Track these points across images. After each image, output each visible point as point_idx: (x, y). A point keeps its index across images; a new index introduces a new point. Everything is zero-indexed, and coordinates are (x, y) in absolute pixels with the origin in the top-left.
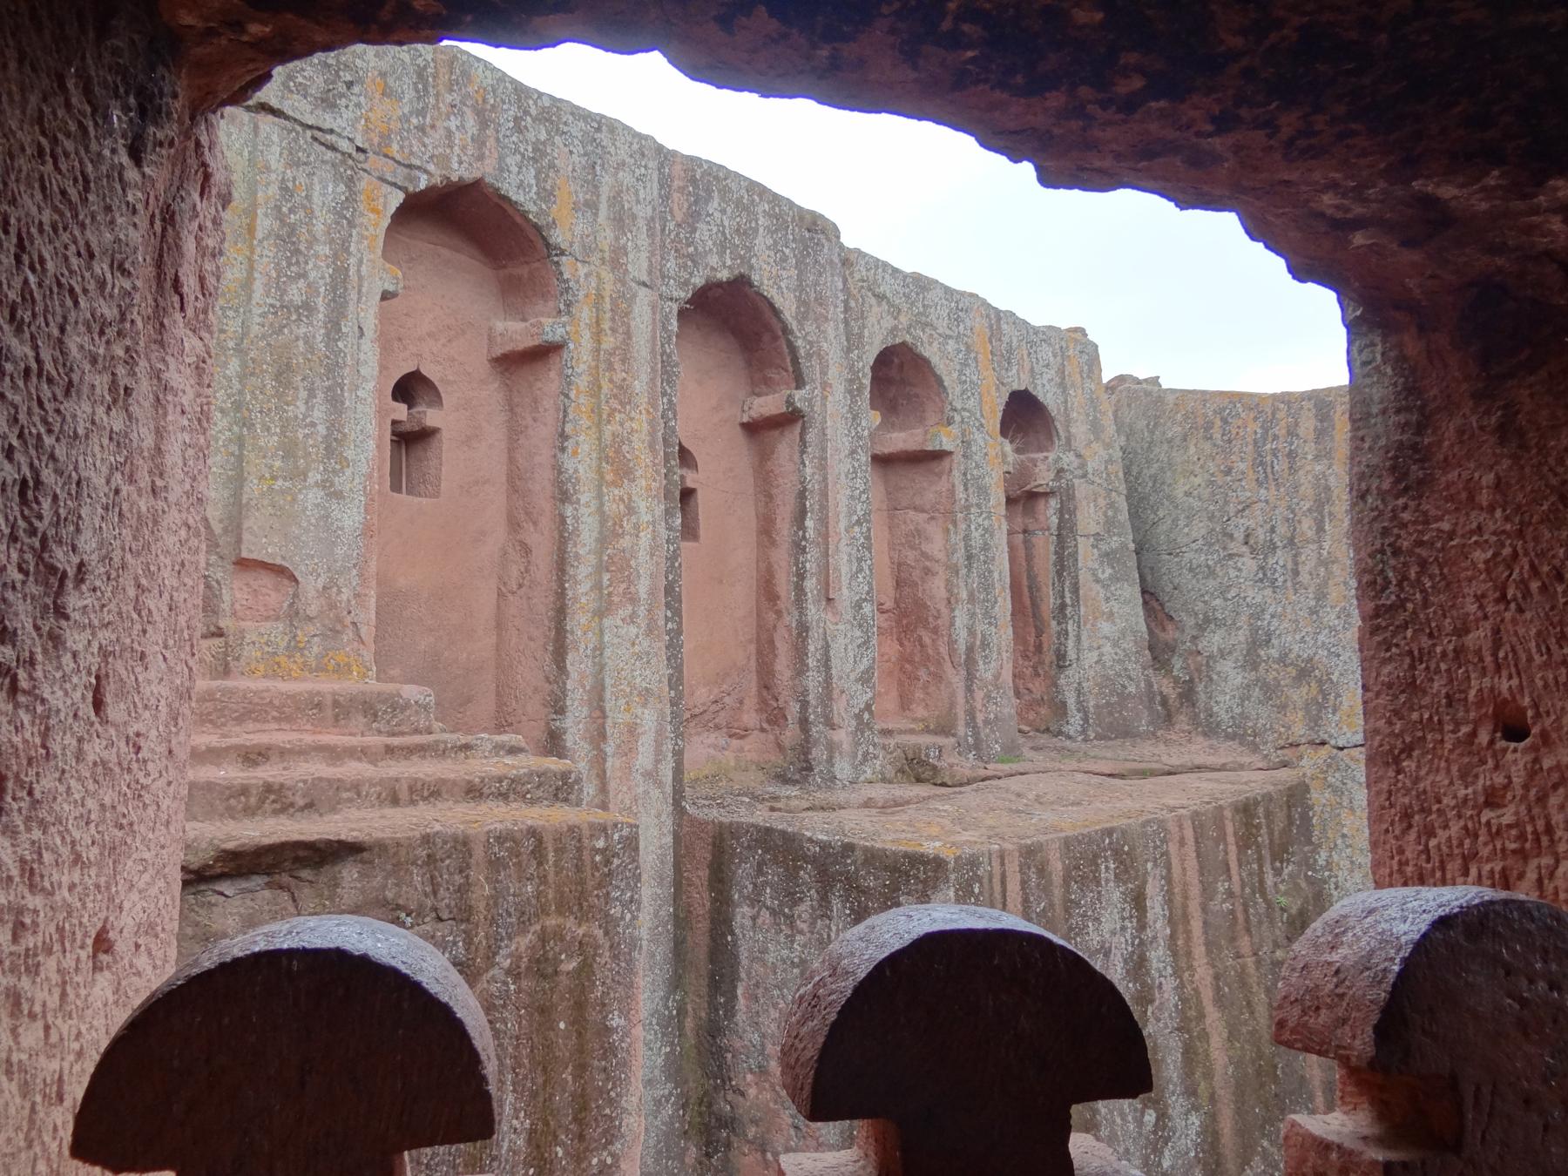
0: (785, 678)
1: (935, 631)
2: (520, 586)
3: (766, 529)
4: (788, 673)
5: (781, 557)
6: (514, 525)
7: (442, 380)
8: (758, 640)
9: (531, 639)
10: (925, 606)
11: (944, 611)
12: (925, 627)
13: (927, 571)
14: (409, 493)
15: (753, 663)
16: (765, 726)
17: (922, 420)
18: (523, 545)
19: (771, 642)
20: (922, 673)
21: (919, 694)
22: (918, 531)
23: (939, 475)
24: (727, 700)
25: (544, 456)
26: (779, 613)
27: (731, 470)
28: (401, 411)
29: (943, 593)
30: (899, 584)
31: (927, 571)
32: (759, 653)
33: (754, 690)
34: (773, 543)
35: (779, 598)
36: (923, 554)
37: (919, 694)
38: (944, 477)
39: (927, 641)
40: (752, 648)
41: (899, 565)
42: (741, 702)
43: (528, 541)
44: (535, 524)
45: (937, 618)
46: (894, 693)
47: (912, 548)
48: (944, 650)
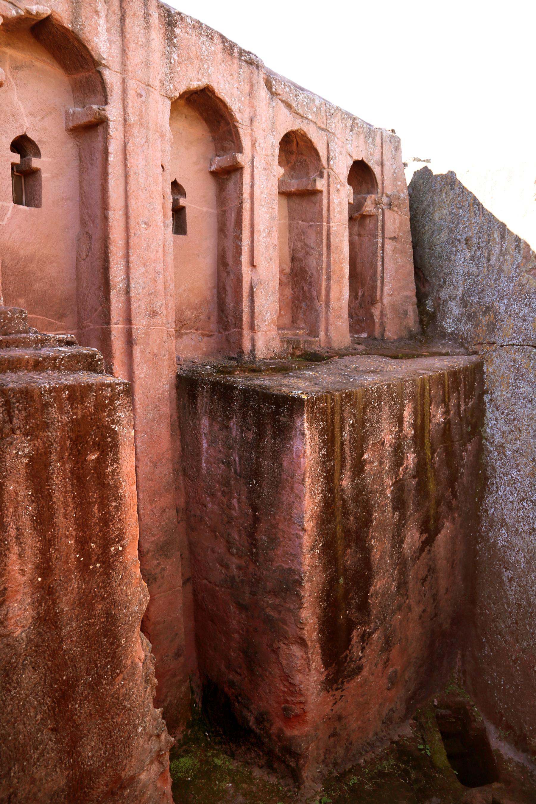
0: (231, 307)
1: (310, 283)
2: (87, 256)
3: (222, 229)
4: (232, 305)
5: (229, 244)
6: (83, 224)
7: (39, 141)
8: (218, 286)
9: (93, 285)
10: (306, 272)
11: (315, 274)
12: (305, 282)
13: (307, 253)
14: (27, 205)
15: (215, 298)
16: (221, 330)
17: (307, 174)
18: (87, 233)
19: (224, 288)
20: (303, 305)
21: (301, 316)
22: (303, 233)
23: (315, 203)
24: (202, 317)
25: (97, 183)
26: (228, 273)
27: (204, 197)
28: (16, 158)
29: (314, 264)
30: (293, 259)
31: (307, 253)
32: (219, 293)
33: (216, 313)
34: (226, 236)
35: (228, 265)
36: (306, 245)
37: (301, 316)
38: (318, 205)
39: (306, 288)
40: (215, 291)
41: (293, 250)
42: (209, 318)
43: (90, 232)
44: (93, 222)
45: (311, 277)
46: (289, 315)
47: (300, 241)
48: (315, 294)
